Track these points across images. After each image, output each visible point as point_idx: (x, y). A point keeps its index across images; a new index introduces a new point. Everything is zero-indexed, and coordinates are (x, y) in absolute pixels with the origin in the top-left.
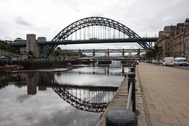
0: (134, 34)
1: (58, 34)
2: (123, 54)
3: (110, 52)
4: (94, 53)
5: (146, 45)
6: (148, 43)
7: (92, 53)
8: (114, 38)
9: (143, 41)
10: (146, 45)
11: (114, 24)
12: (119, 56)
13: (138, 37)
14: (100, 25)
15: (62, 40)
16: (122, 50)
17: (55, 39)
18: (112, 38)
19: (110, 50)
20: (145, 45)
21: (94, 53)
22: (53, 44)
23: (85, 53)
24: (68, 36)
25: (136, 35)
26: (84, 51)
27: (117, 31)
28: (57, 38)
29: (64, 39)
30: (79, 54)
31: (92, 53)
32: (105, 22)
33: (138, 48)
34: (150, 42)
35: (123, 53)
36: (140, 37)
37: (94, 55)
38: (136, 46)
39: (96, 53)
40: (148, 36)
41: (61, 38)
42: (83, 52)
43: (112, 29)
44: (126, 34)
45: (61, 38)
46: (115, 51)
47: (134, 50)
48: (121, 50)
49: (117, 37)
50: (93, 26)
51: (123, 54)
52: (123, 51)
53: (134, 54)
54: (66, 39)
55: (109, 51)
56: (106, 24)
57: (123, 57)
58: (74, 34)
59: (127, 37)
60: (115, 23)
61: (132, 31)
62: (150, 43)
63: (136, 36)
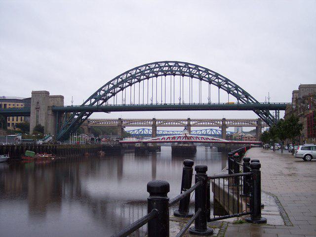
0: (247, 95)
1: (97, 91)
2: (223, 131)
3: (194, 125)
4: (154, 127)
6: (272, 112)
7: (151, 128)
9: (261, 109)
12: (211, 135)
18: (205, 101)
19: (194, 120)
21: (154, 127)
22: (86, 110)
24: (114, 94)
26: (130, 122)
27: (214, 88)
28: (93, 100)
29: (105, 101)
30: (119, 129)
31: (151, 128)
35: (224, 127)
36: (257, 102)
38: (251, 115)
39: (158, 128)
41: (97, 100)
42: (128, 125)
44: (231, 93)
46: (204, 123)
47: (249, 122)
48: (218, 120)
49: (214, 101)
51: (223, 131)
52: (224, 124)
54: (111, 102)
57: (221, 136)
59: (233, 100)
63: (251, 100)
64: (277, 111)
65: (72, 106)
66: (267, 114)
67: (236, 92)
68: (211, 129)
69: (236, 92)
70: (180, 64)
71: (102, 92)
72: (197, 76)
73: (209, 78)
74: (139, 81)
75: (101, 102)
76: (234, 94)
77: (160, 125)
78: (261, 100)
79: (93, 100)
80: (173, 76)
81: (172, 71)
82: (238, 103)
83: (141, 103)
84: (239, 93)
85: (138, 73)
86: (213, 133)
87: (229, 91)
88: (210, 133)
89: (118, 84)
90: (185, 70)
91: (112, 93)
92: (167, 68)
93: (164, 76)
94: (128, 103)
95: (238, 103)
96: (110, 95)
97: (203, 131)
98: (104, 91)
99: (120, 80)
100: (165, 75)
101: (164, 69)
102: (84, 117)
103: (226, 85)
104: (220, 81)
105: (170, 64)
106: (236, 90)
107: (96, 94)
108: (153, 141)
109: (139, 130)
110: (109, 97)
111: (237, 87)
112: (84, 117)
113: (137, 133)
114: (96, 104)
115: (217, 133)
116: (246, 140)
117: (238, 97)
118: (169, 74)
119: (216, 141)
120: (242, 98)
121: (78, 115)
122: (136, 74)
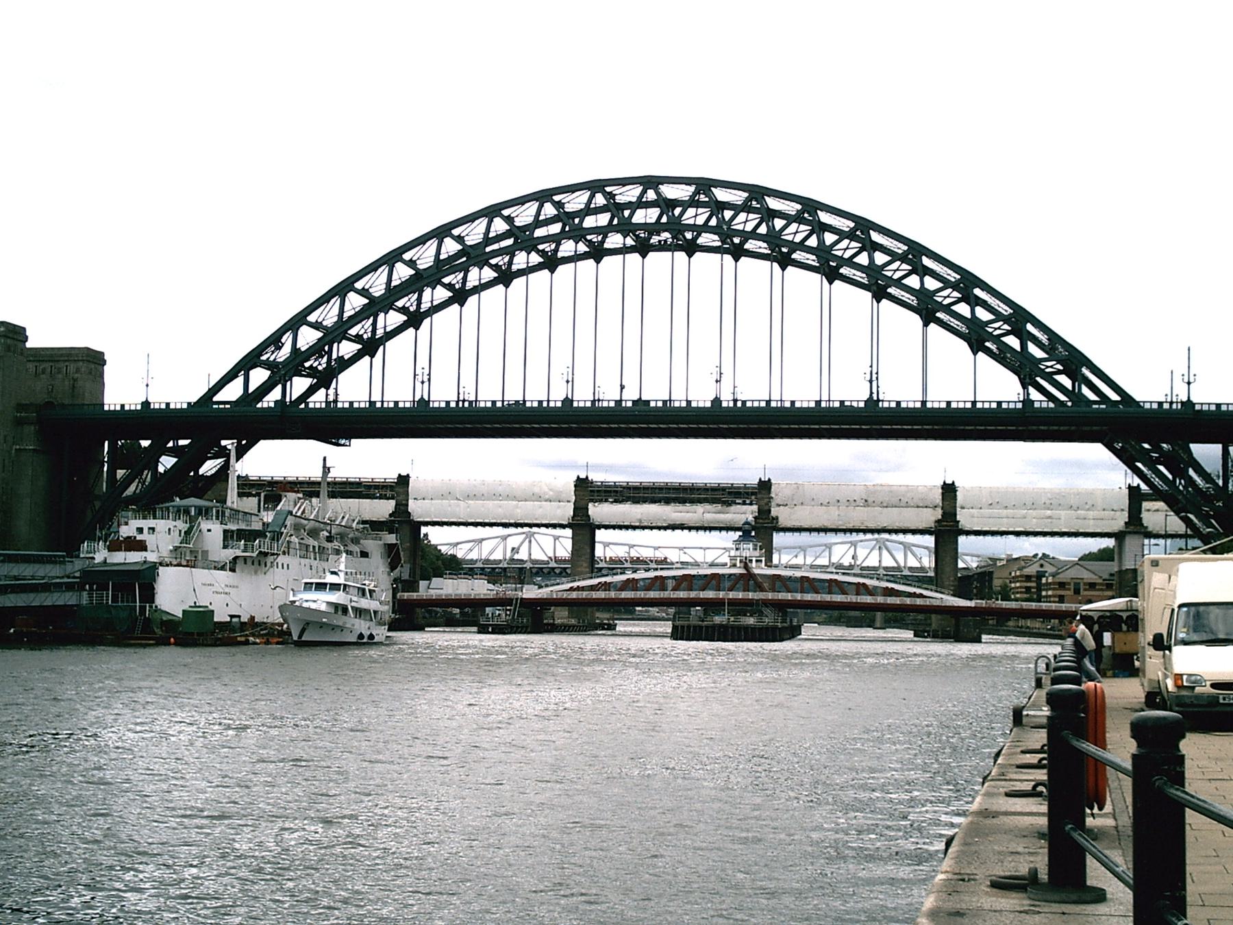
0: (1074, 362)
4: (583, 528)
5: (1191, 472)
10: (1191, 472)
11: (672, 204)
13: (1114, 397)
24: (370, 347)
28: (259, 376)
29: (325, 379)
36: (1126, 398)
41: (281, 374)
44: (988, 352)
45: (296, 364)
56: (689, 235)
57: (935, 582)
61: (1054, 337)
65: (146, 404)
67: (1013, 342)
69: (1013, 342)
70: (721, 195)
71: (308, 337)
72: (811, 259)
73: (873, 271)
74: (505, 277)
75: (300, 385)
76: (1003, 357)
79: (259, 376)
80: (681, 256)
81: (676, 227)
83: (513, 395)
84: (1033, 349)
85: (500, 238)
87: (976, 338)
89: (393, 293)
90: (749, 227)
91: (358, 339)
92: (651, 215)
93: (636, 257)
94: (442, 394)
95: (1027, 402)
96: (347, 349)
98: (316, 326)
99: (402, 272)
101: (640, 217)
102: (209, 467)
103: (963, 309)
104: (931, 284)
105: (670, 191)
106: (1019, 332)
107: (274, 341)
108: (574, 595)
110: (345, 364)
111: (1019, 319)
112: (209, 467)
114: (276, 394)
116: (1061, 599)
117: (1025, 370)
119: (908, 601)
120: (1049, 378)
121: (174, 452)
122: (487, 241)
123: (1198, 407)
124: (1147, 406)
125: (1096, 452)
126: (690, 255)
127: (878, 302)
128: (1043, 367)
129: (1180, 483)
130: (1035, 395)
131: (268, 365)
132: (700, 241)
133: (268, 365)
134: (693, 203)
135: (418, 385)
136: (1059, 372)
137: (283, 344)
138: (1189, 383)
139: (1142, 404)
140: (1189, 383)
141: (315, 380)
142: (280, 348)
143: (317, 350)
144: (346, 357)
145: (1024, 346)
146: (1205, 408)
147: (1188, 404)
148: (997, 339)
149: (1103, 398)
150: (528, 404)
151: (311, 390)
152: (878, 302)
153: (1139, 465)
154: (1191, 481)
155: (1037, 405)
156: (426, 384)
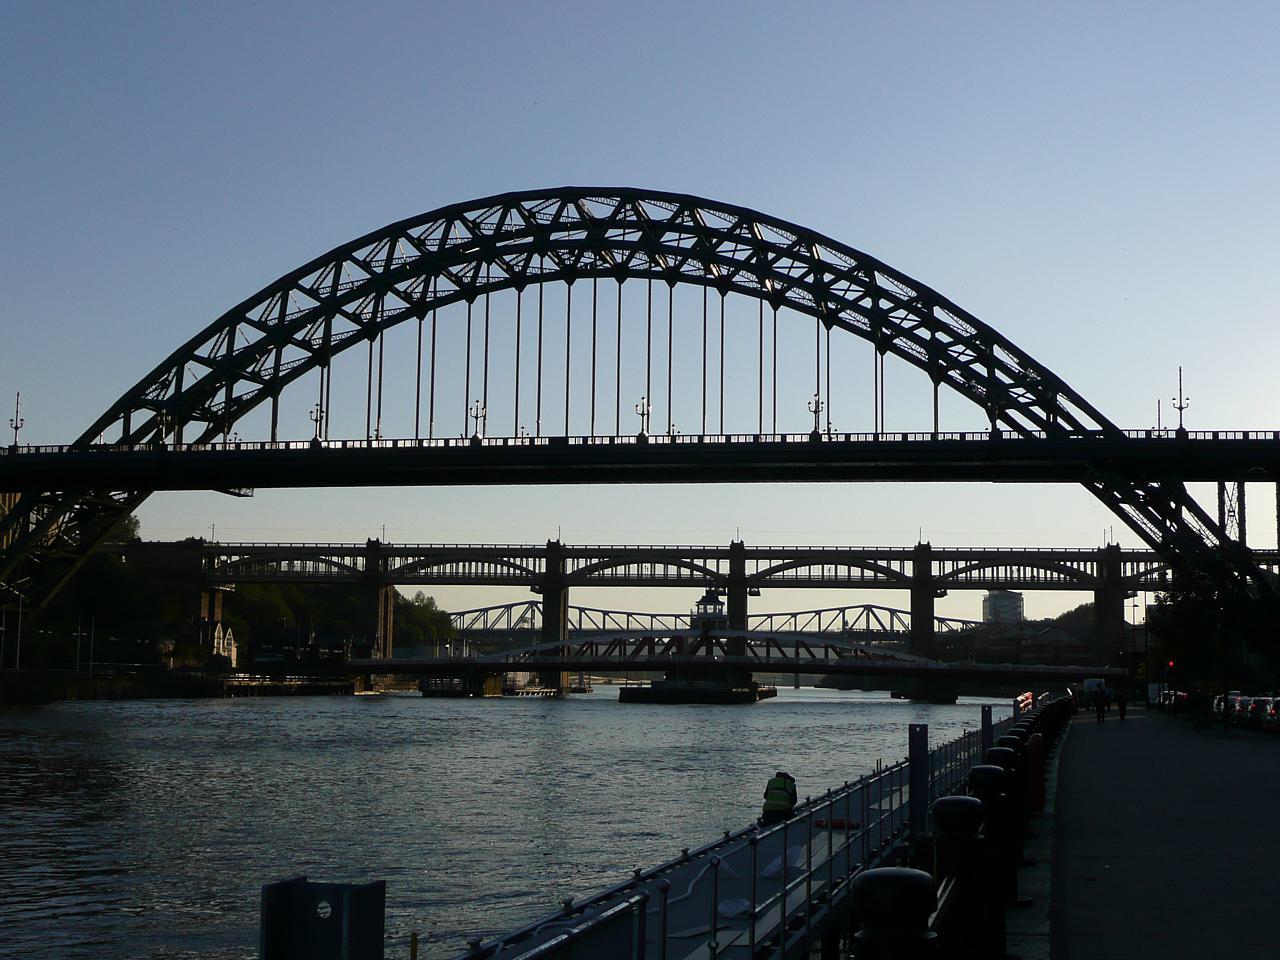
0: (1047, 386)
1: (164, 368)
5: (1186, 514)
6: (1203, 493)
8: (815, 435)
10: (1186, 514)
13: (1091, 425)
14: (605, 273)
15: (193, 431)
16: (902, 556)
17: (118, 425)
18: (796, 426)
20: (1176, 516)
23: (429, 591)
24: (272, 388)
25: (1062, 401)
26: (432, 561)
27: (852, 350)
29: (222, 423)
32: (669, 237)
33: (1095, 542)
34: (1230, 486)
37: (555, 606)
39: (577, 595)
40: (1201, 423)
42: (409, 576)
43: (797, 326)
48: (890, 555)
49: (852, 421)
50: (532, 289)
51: (922, 610)
53: (1043, 606)
54: (250, 431)
55: (751, 567)
58: (349, 364)
59: (967, 419)
60: (766, 234)
61: (1025, 360)
62: (1222, 490)
64: (1230, 486)
66: (1166, 502)
67: (982, 370)
68: (868, 608)
71: (194, 373)
77: (583, 578)
78: (1134, 417)
79: (141, 417)
80: (660, 285)
82: (996, 433)
84: (999, 374)
86: (875, 626)
87: (937, 366)
88: (861, 625)
95: (996, 433)
97: (826, 618)
100: (569, 274)
103: (924, 333)
104: (884, 304)
107: (155, 378)
109: (509, 607)
110: (239, 407)
113: (502, 625)
115: (898, 627)
117: (995, 401)
118: (593, 272)
120: (1024, 409)
123: (1191, 436)
124: (1133, 435)
125: (1075, 494)
126: (621, 281)
127: (828, 328)
128: (1028, 395)
129: (1172, 525)
130: (1001, 425)
131: (154, 405)
132: (736, 279)
133: (154, 405)
134: (788, 252)
135: (472, 421)
136: (1033, 403)
137: (171, 382)
138: (1181, 408)
139: (1126, 433)
140: (1181, 408)
141: (212, 425)
142: (168, 387)
143: (205, 389)
144: (245, 398)
145: (991, 372)
146: (1200, 437)
147: (1182, 432)
148: (964, 368)
149: (1078, 428)
150: (571, 442)
151: (205, 438)
152: (828, 328)
153: (1125, 507)
154: (1183, 526)
155: (1006, 436)
156: (481, 420)
